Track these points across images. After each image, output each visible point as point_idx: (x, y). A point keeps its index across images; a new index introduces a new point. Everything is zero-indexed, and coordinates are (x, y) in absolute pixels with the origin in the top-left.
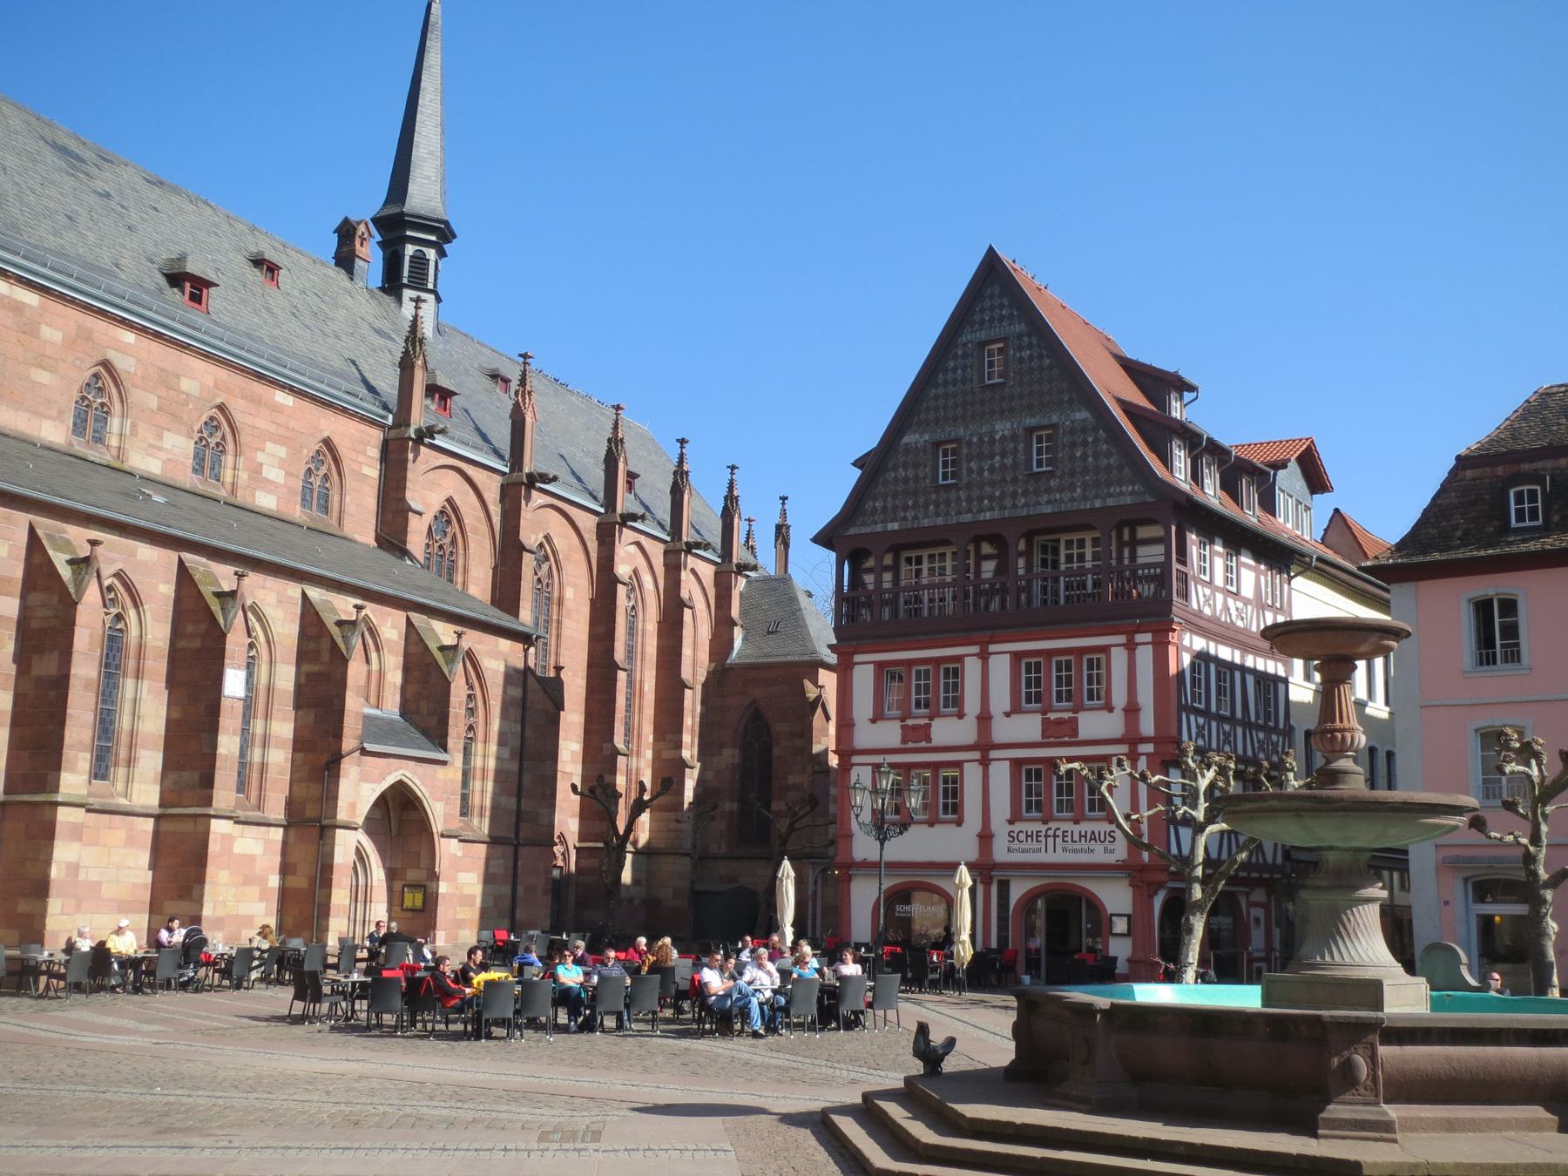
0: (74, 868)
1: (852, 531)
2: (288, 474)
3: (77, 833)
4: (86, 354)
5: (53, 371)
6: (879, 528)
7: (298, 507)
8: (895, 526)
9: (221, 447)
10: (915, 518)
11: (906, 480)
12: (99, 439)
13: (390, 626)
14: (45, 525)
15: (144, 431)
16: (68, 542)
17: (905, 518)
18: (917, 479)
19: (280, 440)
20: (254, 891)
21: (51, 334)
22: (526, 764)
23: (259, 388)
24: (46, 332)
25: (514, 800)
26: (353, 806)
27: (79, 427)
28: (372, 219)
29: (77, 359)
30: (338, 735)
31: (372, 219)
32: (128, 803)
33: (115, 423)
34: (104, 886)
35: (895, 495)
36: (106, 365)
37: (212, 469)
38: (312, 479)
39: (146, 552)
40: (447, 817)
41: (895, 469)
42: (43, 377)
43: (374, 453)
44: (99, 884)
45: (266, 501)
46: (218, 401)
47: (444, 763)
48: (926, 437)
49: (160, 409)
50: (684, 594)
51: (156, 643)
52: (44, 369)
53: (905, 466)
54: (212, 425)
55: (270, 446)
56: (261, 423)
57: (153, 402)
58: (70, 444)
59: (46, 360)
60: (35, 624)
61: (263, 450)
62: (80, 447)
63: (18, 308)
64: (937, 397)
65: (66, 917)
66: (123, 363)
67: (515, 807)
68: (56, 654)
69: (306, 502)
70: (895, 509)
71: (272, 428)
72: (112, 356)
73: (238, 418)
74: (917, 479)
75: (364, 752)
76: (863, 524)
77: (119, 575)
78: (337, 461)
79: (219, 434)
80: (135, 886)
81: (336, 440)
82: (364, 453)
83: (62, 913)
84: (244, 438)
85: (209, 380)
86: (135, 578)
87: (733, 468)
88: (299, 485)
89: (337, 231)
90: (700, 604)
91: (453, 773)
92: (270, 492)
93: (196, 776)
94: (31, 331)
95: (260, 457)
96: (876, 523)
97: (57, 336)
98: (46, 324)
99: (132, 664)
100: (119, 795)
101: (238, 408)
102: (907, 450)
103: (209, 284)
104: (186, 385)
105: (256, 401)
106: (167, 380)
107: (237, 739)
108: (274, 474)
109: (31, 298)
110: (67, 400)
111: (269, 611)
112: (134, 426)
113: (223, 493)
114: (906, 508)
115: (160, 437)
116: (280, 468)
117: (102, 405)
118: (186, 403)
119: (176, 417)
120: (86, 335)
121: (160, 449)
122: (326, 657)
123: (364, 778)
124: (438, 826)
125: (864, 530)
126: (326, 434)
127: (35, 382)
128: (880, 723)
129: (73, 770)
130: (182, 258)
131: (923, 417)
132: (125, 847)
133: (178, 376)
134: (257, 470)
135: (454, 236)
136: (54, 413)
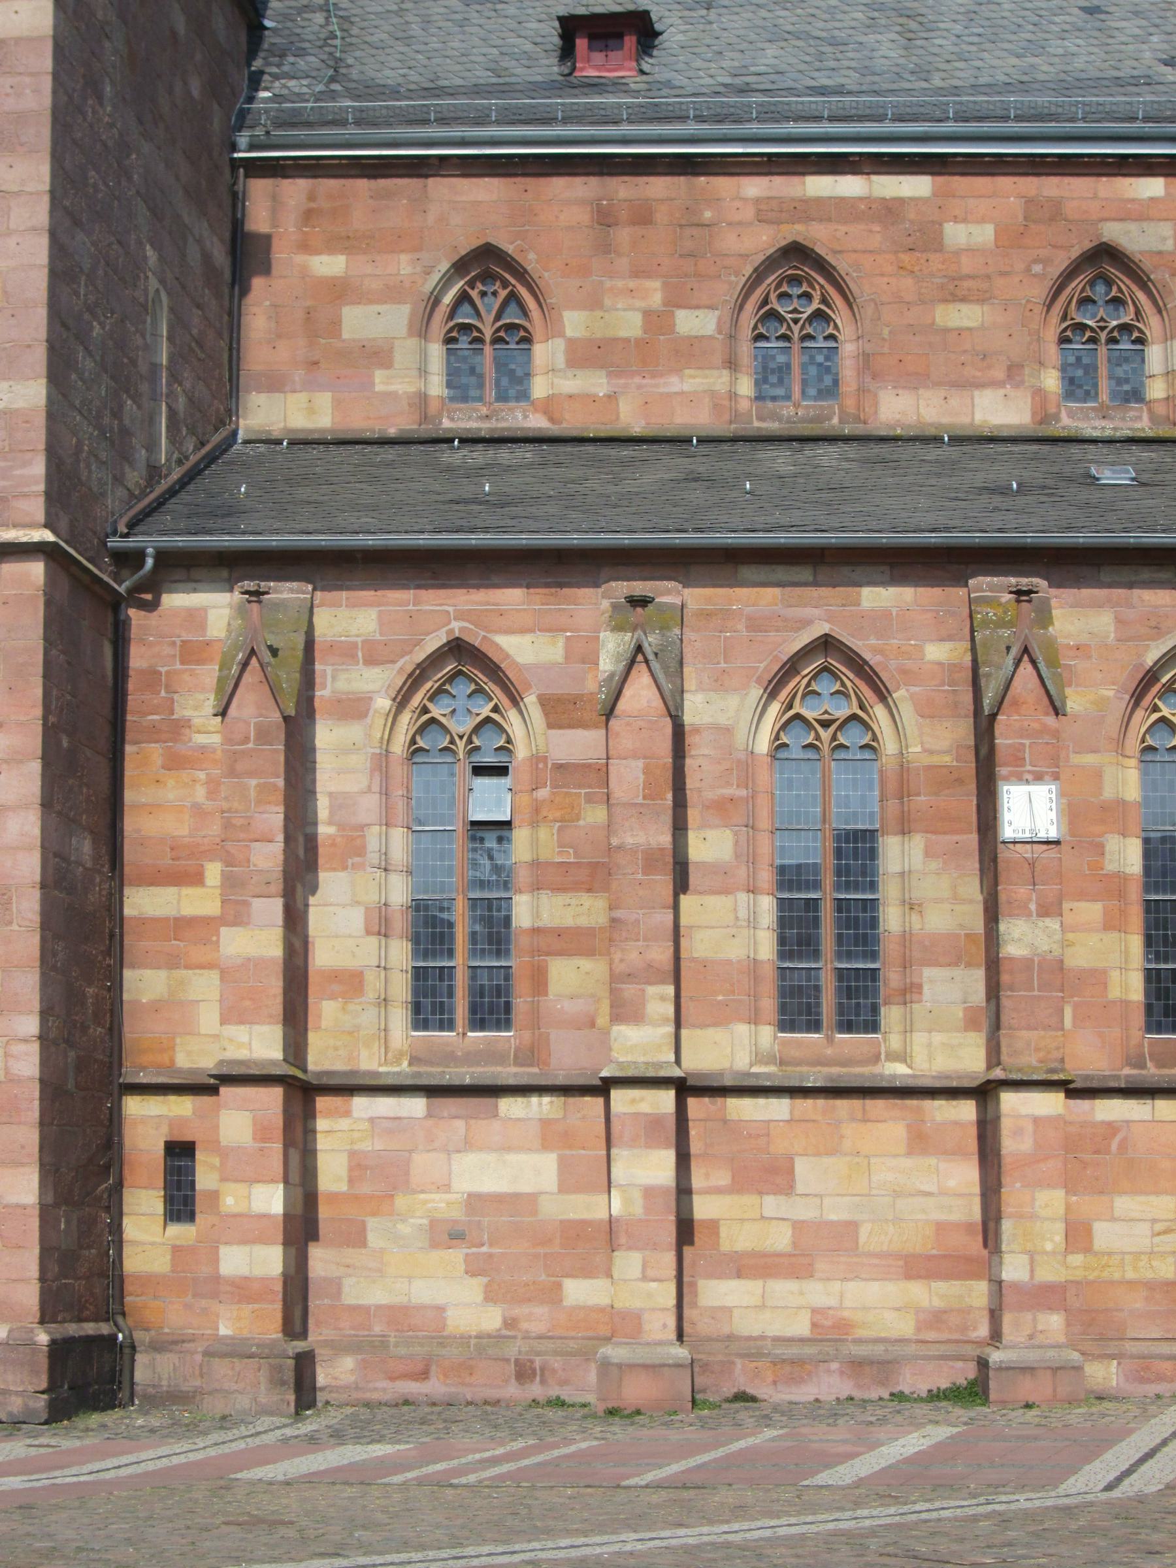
4: (1054, 247)
5: (982, 298)
24: (956, 234)
29: (1036, 261)
32: (908, 1071)
44: (852, 1227)
51: (927, 760)
52: (963, 300)
59: (966, 284)
63: (890, 210)
65: (654, 1285)
80: (941, 1228)
83: (645, 1278)
97: (984, 234)
98: (955, 219)
100: (893, 1057)
109: (916, 186)
127: (946, 330)
132: (910, 1153)
136: (999, 373)
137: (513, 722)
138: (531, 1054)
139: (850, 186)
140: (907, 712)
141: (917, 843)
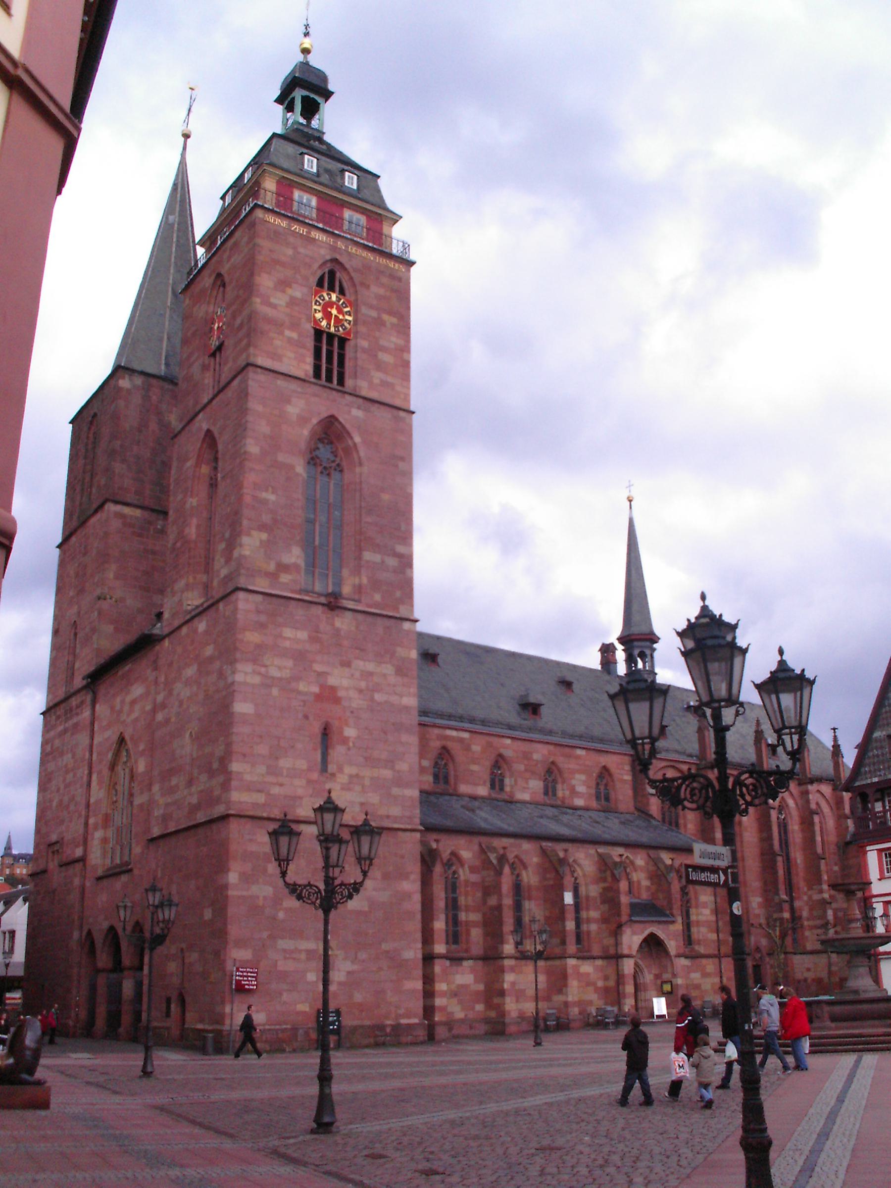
0: (513, 984)
1: (857, 784)
2: (588, 787)
3: (512, 969)
6: (869, 781)
7: (595, 802)
8: (875, 780)
9: (555, 781)
10: (885, 774)
11: (878, 756)
12: (502, 789)
13: (640, 860)
14: (484, 840)
15: (520, 782)
16: (494, 848)
17: (881, 775)
18: (883, 754)
19: (580, 772)
20: (591, 988)
21: (476, 748)
22: (719, 916)
23: (567, 750)
25: (716, 935)
26: (630, 948)
27: (493, 786)
28: (618, 639)
30: (619, 914)
31: (618, 639)
33: (507, 781)
34: (527, 991)
35: (874, 764)
36: (500, 755)
37: (553, 791)
38: (600, 787)
39: (526, 846)
40: (678, 947)
41: (872, 750)
42: (475, 768)
43: (627, 768)
45: (579, 802)
46: (551, 760)
47: (673, 922)
48: (884, 733)
49: (526, 770)
50: (813, 806)
53: (877, 748)
54: (549, 771)
55: (577, 776)
56: (572, 766)
57: (522, 767)
58: (490, 794)
60: (486, 884)
61: (574, 778)
62: (494, 795)
63: (461, 740)
64: (886, 712)
66: (508, 753)
67: (716, 938)
68: (496, 897)
69: (598, 798)
70: (875, 770)
71: (577, 767)
72: (503, 751)
73: (561, 765)
74: (883, 754)
75: (631, 921)
76: (862, 780)
77: (516, 857)
78: (610, 775)
79: (554, 774)
81: (609, 765)
82: (623, 769)
84: (566, 775)
85: (545, 752)
86: (524, 857)
87: (834, 729)
88: (593, 791)
89: (600, 650)
90: (826, 809)
91: (678, 926)
92: (579, 797)
93: (559, 941)
94: (467, 748)
95: (574, 782)
96: (867, 778)
99: (526, 894)
101: (561, 761)
102: (876, 740)
103: (540, 705)
104: (536, 756)
105: (569, 756)
106: (527, 756)
107: (574, 923)
108: (581, 789)
109: (466, 735)
110: (486, 776)
111: (582, 862)
112: (516, 781)
113: (559, 803)
114: (880, 770)
115: (527, 783)
116: (584, 785)
117: (501, 774)
118: (536, 765)
119: (533, 773)
120: (490, 745)
121: (528, 788)
122: (609, 879)
123: (634, 933)
124: (673, 951)
125: (864, 782)
126: (603, 764)
128: (883, 881)
129: (508, 943)
130: (527, 696)
131: (881, 723)
133: (531, 753)
134: (573, 790)
135: (659, 639)
136: (482, 782)
137: (461, 871)
138: (467, 951)
139: (454, 733)
140: (530, 873)
141: (533, 903)
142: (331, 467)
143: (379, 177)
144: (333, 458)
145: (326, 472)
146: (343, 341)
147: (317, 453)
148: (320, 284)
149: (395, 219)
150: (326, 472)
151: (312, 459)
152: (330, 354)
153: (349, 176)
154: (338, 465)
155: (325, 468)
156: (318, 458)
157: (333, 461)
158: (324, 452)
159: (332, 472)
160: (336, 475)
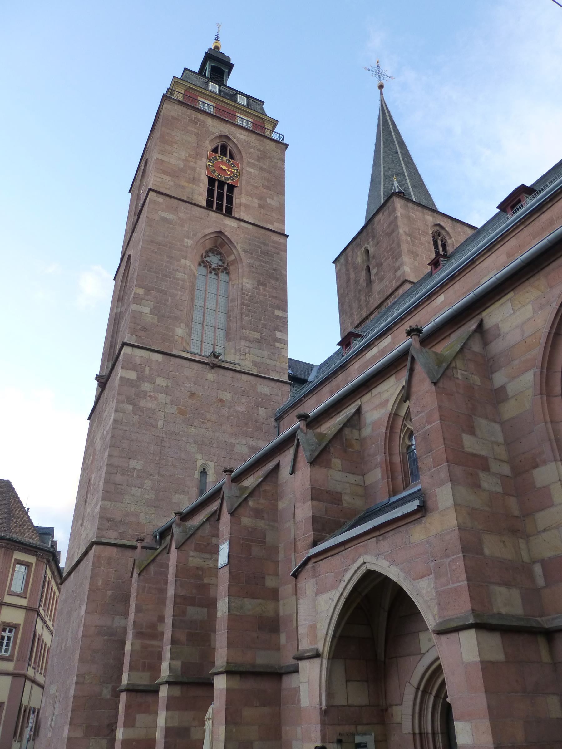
142: (219, 269)
143: (263, 102)
144: (220, 263)
145: (215, 271)
146: (231, 188)
147: (208, 259)
148: (215, 150)
149: (275, 123)
150: (213, 272)
151: (203, 262)
152: (220, 197)
153: (240, 96)
154: (225, 269)
155: (214, 269)
156: (208, 262)
157: (221, 266)
158: (214, 260)
159: (220, 272)
160: (223, 276)
